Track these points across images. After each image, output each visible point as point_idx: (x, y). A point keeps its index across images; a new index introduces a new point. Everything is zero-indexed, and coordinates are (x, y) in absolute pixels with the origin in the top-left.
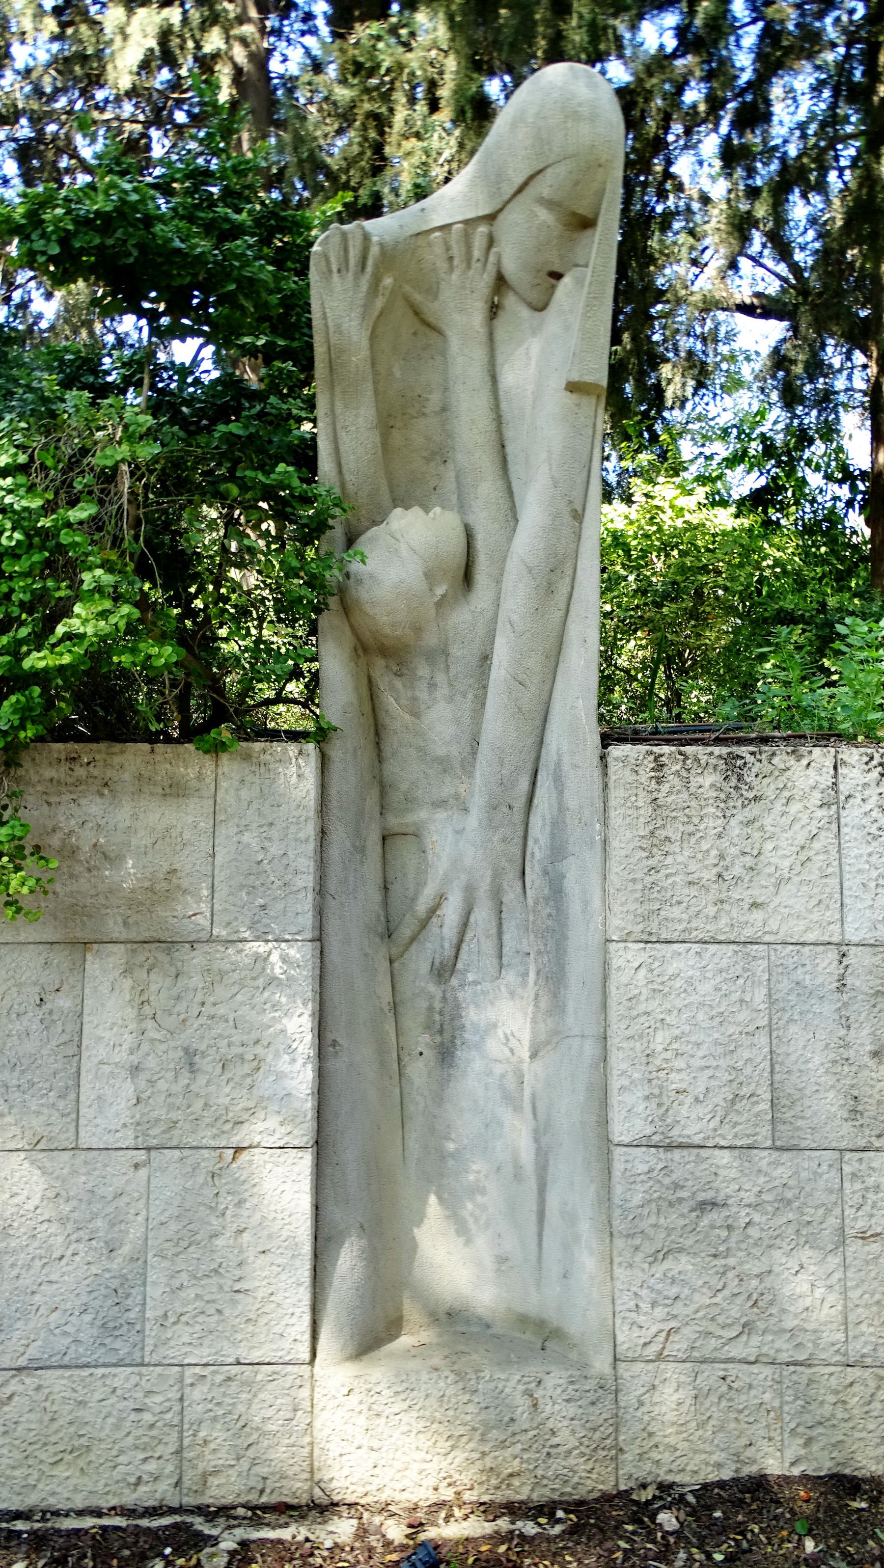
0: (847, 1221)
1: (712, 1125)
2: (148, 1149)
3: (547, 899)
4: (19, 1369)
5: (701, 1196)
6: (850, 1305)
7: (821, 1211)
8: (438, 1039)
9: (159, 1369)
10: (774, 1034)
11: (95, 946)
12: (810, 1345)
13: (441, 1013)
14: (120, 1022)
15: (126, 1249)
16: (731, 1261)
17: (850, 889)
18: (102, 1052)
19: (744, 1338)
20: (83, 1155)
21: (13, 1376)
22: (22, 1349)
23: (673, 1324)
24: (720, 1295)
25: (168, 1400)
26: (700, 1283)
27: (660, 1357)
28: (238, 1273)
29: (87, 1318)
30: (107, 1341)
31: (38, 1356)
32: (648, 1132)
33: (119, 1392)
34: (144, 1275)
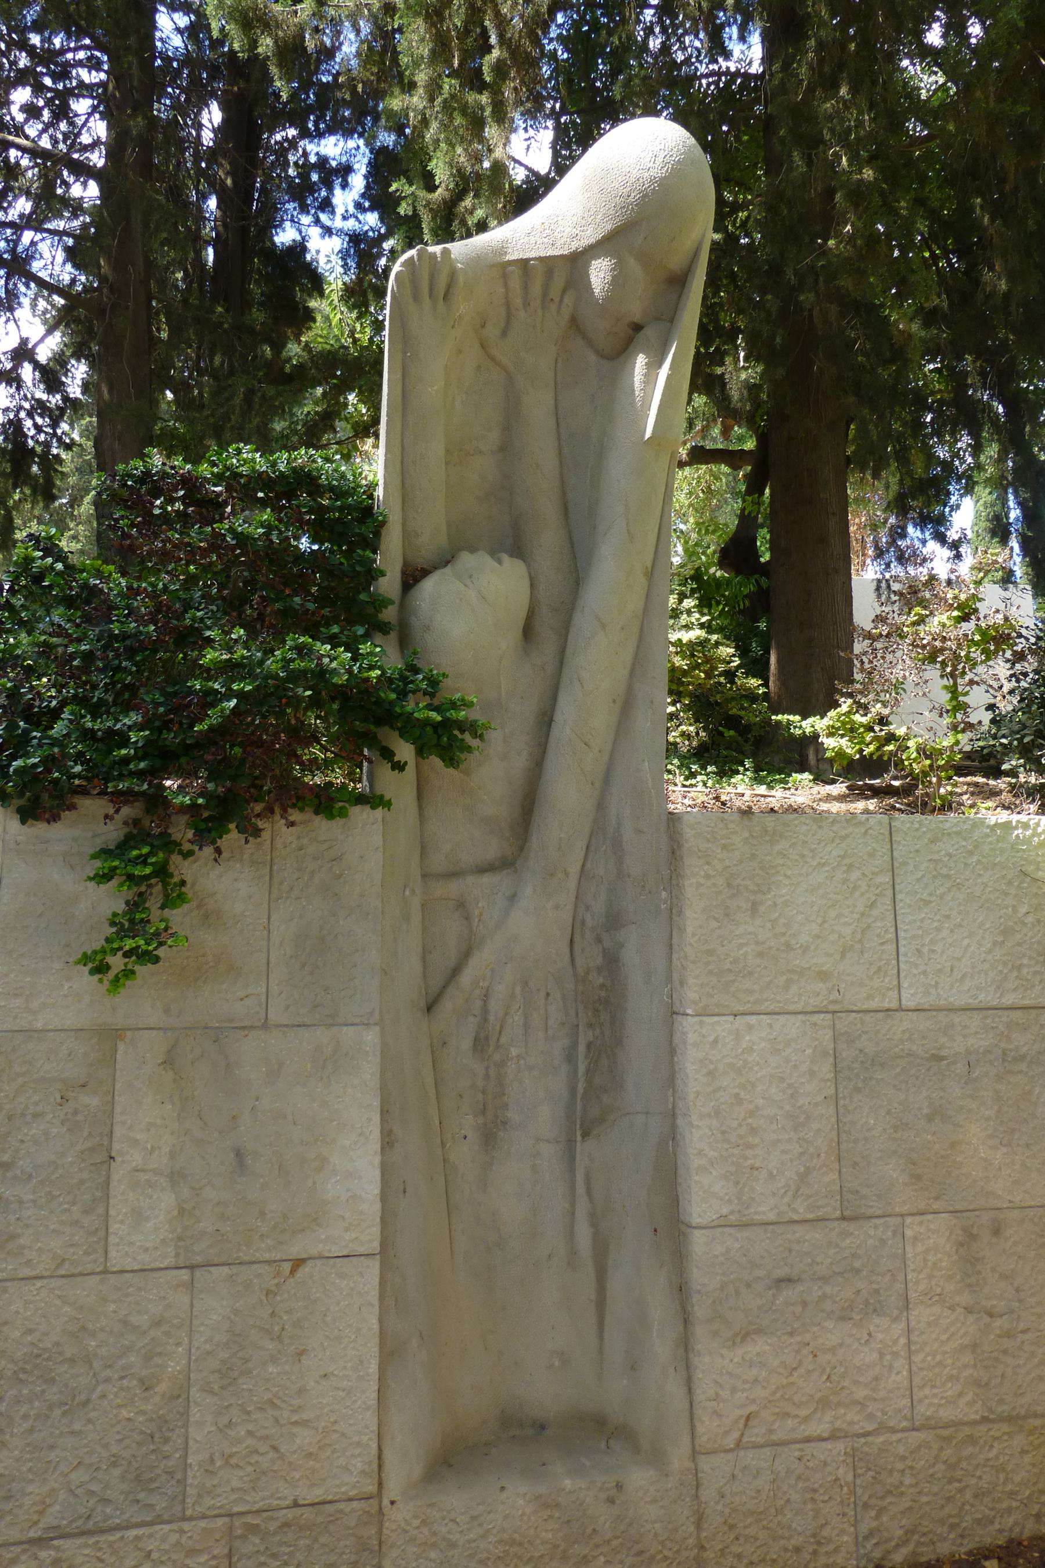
0: (910, 1285)
1: (786, 1200)
2: (192, 1268)
3: (599, 970)
4: (32, 1542)
5: (779, 1273)
6: (914, 1368)
7: (888, 1278)
8: (481, 1120)
9: (203, 1524)
10: (841, 1103)
11: (129, 1034)
12: (879, 1414)
13: (484, 1092)
14: (159, 1121)
15: (162, 1387)
16: (808, 1337)
17: (906, 955)
18: (136, 1158)
19: (818, 1415)
20: (113, 1279)
21: (24, 1551)
22: (35, 1517)
23: (753, 1408)
24: (796, 1374)
25: (214, 1557)
26: (776, 1363)
27: (739, 1445)
28: (296, 1402)
29: (117, 1472)
30: (141, 1496)
31: (55, 1523)
32: (725, 1211)
33: (155, 1555)
34: (186, 1413)
